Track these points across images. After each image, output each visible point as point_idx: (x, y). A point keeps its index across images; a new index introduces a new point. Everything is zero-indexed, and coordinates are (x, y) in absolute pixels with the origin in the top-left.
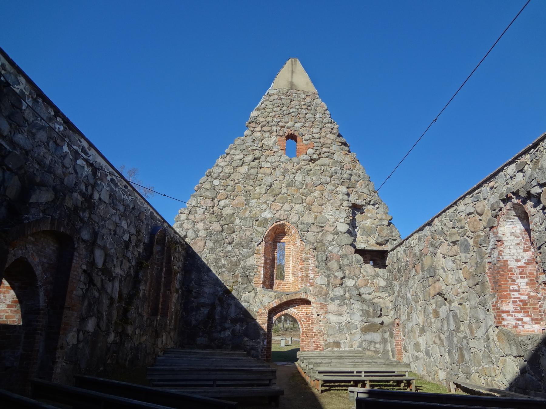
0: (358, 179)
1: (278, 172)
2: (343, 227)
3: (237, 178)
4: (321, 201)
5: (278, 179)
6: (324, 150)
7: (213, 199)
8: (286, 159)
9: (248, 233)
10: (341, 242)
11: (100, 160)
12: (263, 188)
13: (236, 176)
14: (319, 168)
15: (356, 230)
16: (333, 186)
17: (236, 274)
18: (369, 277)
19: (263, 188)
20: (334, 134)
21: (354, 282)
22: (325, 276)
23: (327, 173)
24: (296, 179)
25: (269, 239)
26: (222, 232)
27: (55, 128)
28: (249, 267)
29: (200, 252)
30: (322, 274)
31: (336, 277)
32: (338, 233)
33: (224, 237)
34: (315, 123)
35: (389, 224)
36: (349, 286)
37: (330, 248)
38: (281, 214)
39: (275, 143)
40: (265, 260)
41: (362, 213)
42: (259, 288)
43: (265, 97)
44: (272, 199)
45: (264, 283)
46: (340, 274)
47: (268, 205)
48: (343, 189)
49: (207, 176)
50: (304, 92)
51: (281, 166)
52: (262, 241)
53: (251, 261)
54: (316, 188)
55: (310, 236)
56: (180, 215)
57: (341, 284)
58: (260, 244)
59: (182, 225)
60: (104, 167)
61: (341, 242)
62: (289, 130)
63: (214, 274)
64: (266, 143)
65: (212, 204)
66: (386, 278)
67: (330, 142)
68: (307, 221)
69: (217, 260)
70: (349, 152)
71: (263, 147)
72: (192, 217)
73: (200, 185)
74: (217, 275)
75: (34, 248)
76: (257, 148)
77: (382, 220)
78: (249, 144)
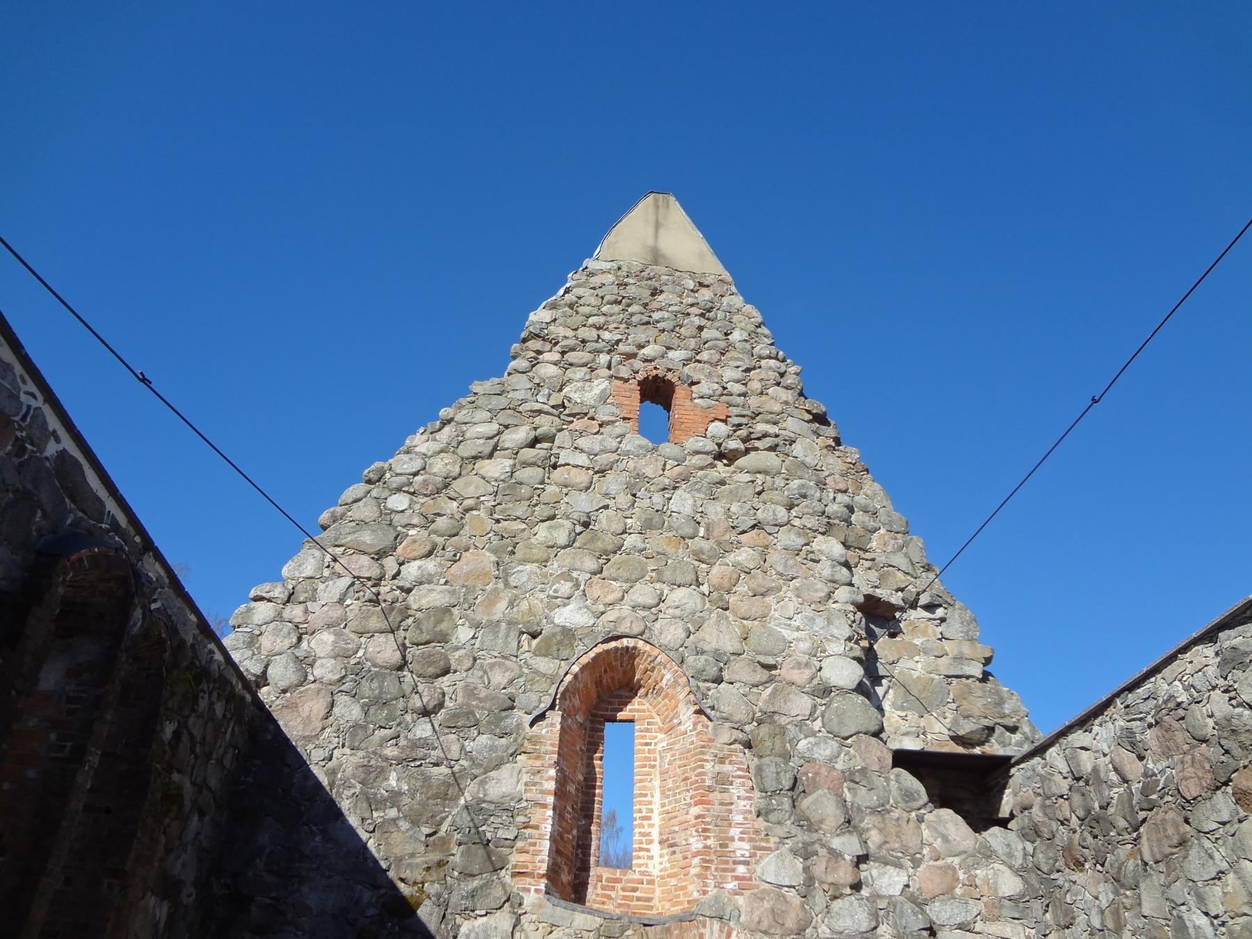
0: (872, 524)
1: (613, 483)
2: (845, 673)
3: (471, 491)
4: (760, 580)
5: (611, 503)
6: (761, 427)
7: (379, 555)
8: (641, 447)
9: (499, 678)
10: (841, 723)
12: (562, 526)
13: (468, 487)
14: (748, 477)
15: (880, 691)
16: (799, 535)
17: (442, 833)
18: (956, 861)
19: (562, 526)
20: (787, 388)
21: (904, 879)
22: (795, 852)
23: (776, 496)
24: (673, 505)
25: (577, 702)
26: (400, 668)
28: (498, 805)
29: (308, 739)
30: (783, 840)
31: (835, 855)
32: (825, 691)
33: (407, 688)
34: (728, 355)
35: (985, 677)
36: (884, 892)
37: (803, 745)
38: (624, 618)
39: (603, 398)
40: (562, 781)
41: (893, 635)
42: (533, 893)
43: (576, 277)
44: (591, 564)
45: (552, 874)
46: (849, 846)
47: (577, 585)
48: (831, 547)
49: (369, 482)
50: (692, 274)
51: (622, 466)
52: (552, 707)
53: (504, 783)
54: (743, 538)
55: (728, 697)
56: (253, 604)
57: (856, 887)
58: (542, 717)
59: (252, 641)
61: (841, 723)
62: (650, 366)
63: (351, 830)
64: (576, 397)
65: (375, 572)
66: (1018, 862)
67: (777, 408)
68: (714, 645)
69: (371, 773)
70: (838, 441)
71: (564, 407)
72: (295, 612)
73: (339, 510)
74: (364, 836)
76: (546, 408)
77: (959, 659)
78: (519, 395)
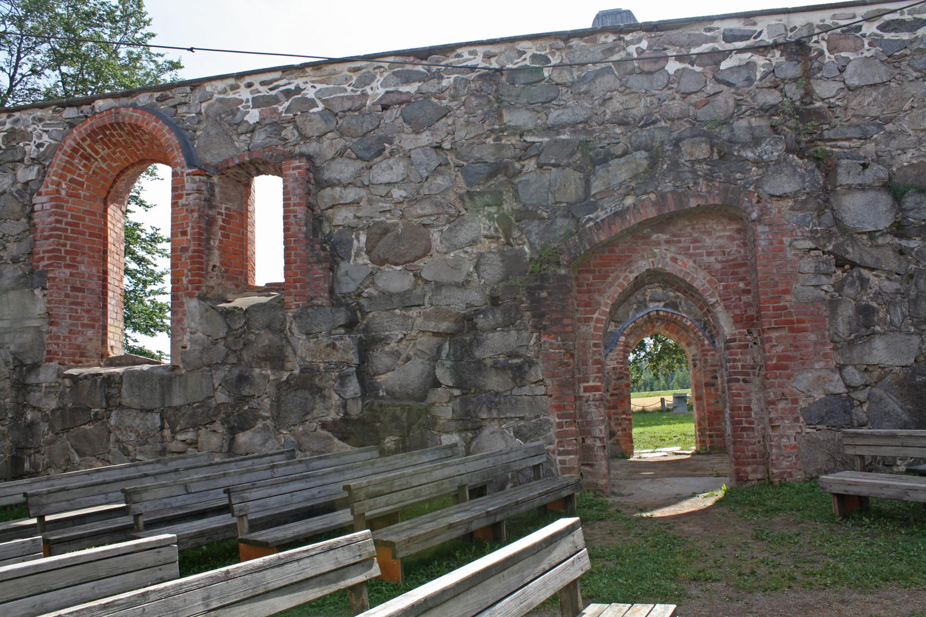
11: (799, 20)
27: (629, 54)
60: (829, 22)
75: (673, 249)
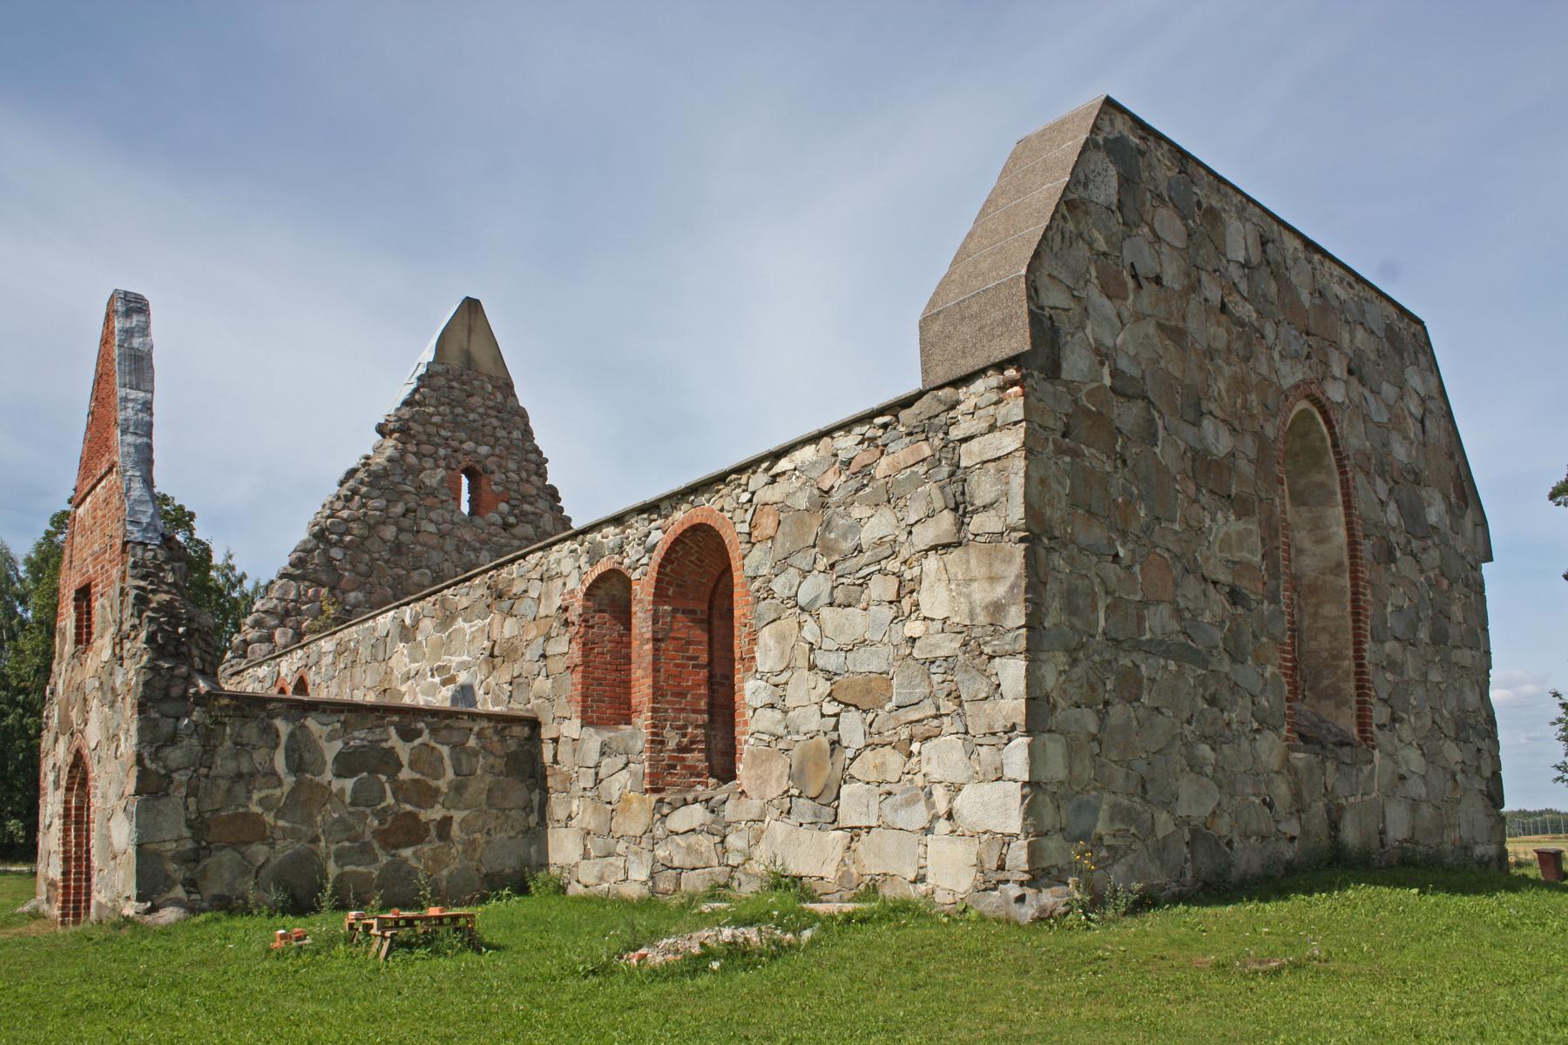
50: (490, 378)
64: (427, 481)
67: (534, 492)
